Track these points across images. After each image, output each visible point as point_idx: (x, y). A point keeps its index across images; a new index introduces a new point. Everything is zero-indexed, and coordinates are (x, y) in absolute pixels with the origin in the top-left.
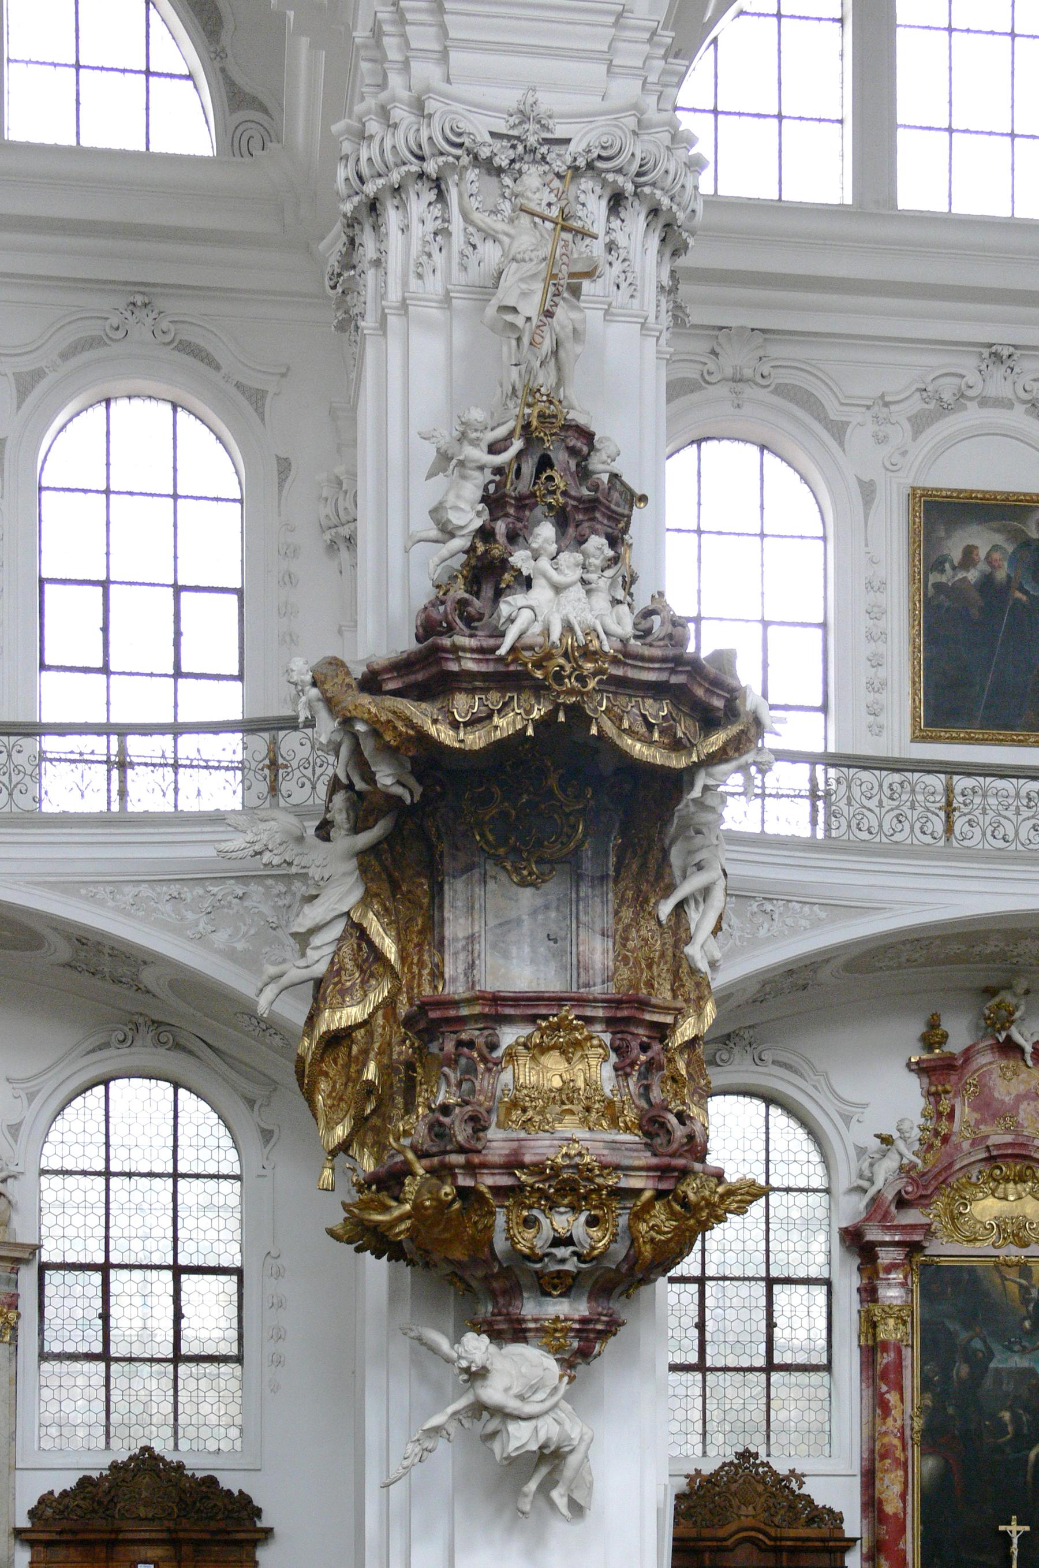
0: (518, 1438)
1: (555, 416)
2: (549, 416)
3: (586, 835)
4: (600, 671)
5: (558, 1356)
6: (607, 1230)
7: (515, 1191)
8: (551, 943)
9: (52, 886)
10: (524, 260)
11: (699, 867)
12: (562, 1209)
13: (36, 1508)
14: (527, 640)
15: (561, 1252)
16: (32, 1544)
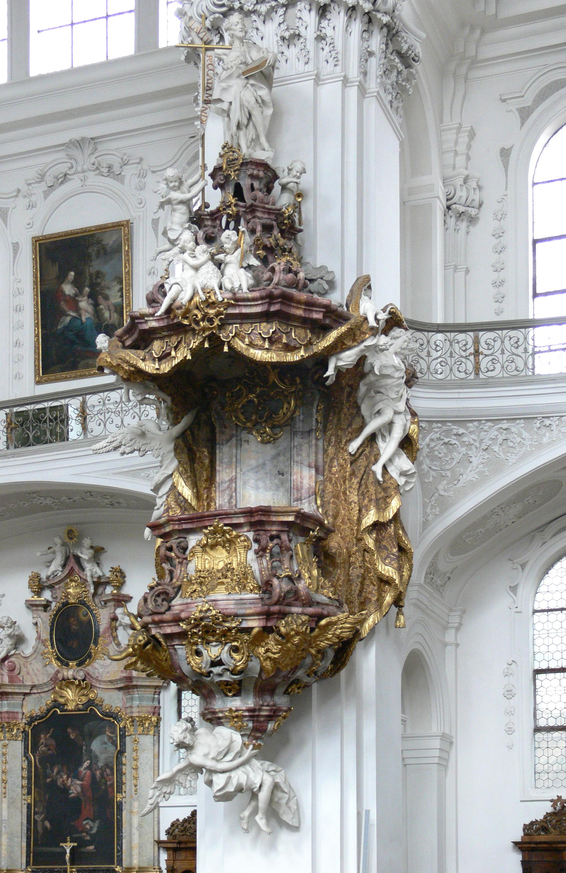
0: (218, 784)
1: (237, 159)
2: (233, 160)
3: (296, 406)
4: (218, 314)
5: (242, 733)
6: (243, 654)
7: (182, 635)
8: (281, 476)
9: (126, 473)
10: (228, 69)
11: (379, 412)
12: (214, 644)
13: (170, 828)
14: (177, 303)
15: (217, 670)
16: (167, 849)
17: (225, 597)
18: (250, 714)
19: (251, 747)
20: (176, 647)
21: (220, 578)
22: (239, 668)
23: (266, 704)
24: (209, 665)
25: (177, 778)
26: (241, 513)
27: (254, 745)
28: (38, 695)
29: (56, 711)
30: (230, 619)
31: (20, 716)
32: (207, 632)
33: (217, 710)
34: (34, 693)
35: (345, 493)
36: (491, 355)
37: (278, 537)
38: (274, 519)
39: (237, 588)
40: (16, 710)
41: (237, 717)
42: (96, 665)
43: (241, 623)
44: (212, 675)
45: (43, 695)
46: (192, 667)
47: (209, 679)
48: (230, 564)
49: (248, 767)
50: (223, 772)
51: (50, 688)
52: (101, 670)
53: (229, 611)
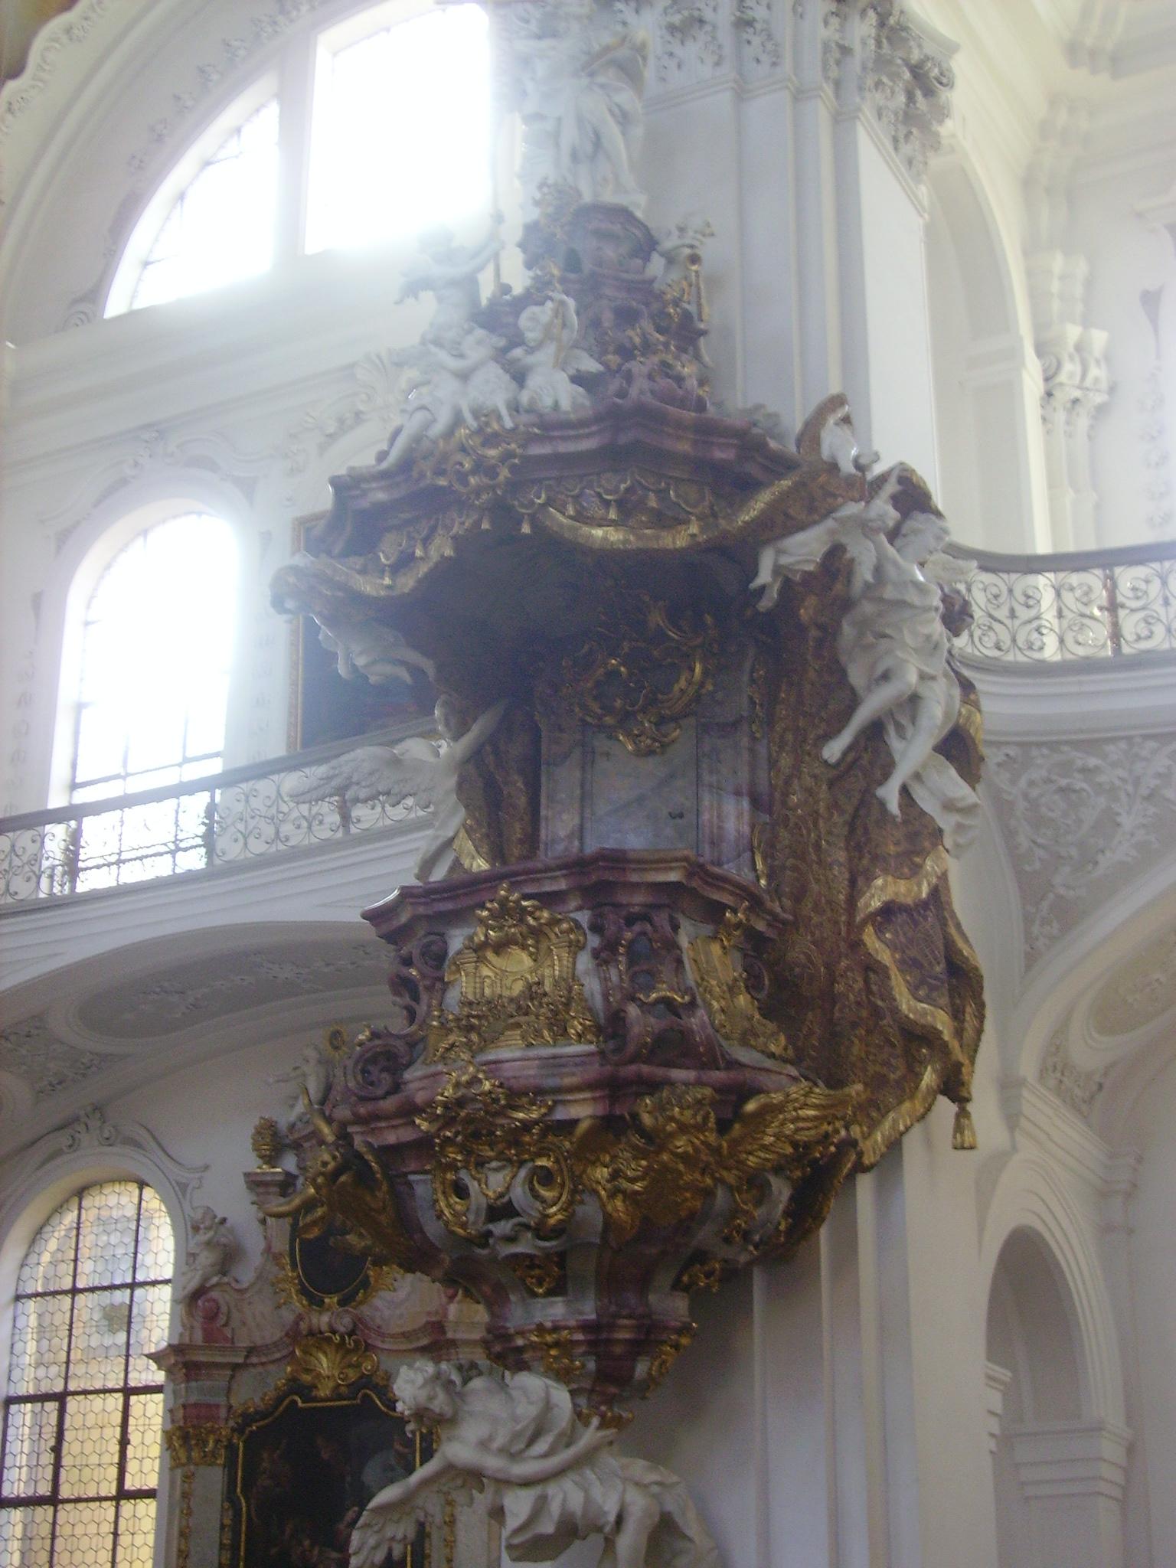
3: (705, 673)
5: (574, 1386)
6: (563, 1185)
8: (679, 821)
11: (886, 677)
12: (494, 1164)
15: (502, 1227)
17: (518, 1054)
18: (591, 1337)
19: (595, 1421)
20: (412, 1177)
21: (512, 1016)
22: (552, 1221)
23: (625, 1312)
24: (482, 1218)
25: (419, 1502)
26: (559, 868)
27: (603, 1416)
28: (260, 1369)
29: (295, 1402)
30: (525, 1100)
31: (223, 1413)
32: (476, 1136)
33: (512, 1331)
34: (254, 1365)
35: (817, 846)
36: (1143, 608)
37: (645, 917)
38: (634, 878)
39: (546, 1033)
40: (213, 1400)
41: (557, 1344)
42: (377, 1302)
43: (551, 1109)
44: (491, 1241)
45: (271, 1367)
46: (447, 1223)
47: (485, 1252)
48: (538, 984)
49: (589, 1473)
50: (526, 1483)
51: (285, 1352)
52: (387, 1313)
53: (522, 1082)
